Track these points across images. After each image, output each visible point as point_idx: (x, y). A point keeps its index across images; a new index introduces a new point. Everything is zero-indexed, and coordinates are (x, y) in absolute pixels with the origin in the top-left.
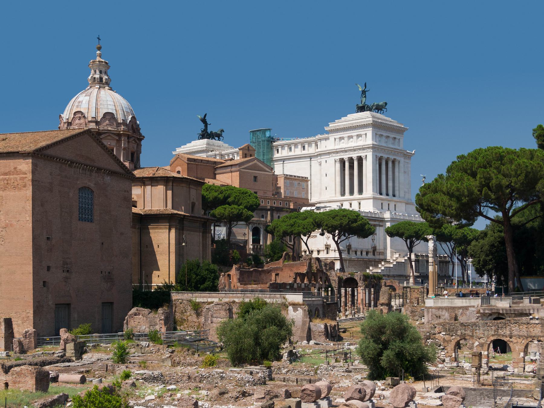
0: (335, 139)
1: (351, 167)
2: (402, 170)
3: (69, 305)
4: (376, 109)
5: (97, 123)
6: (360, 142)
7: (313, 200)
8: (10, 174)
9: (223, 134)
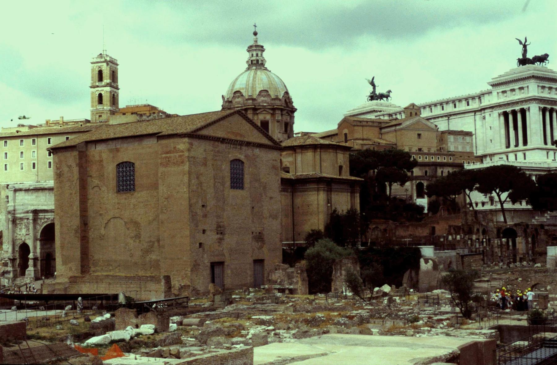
0: (498, 93)
5: (253, 100)
8: (171, 153)
9: (391, 94)
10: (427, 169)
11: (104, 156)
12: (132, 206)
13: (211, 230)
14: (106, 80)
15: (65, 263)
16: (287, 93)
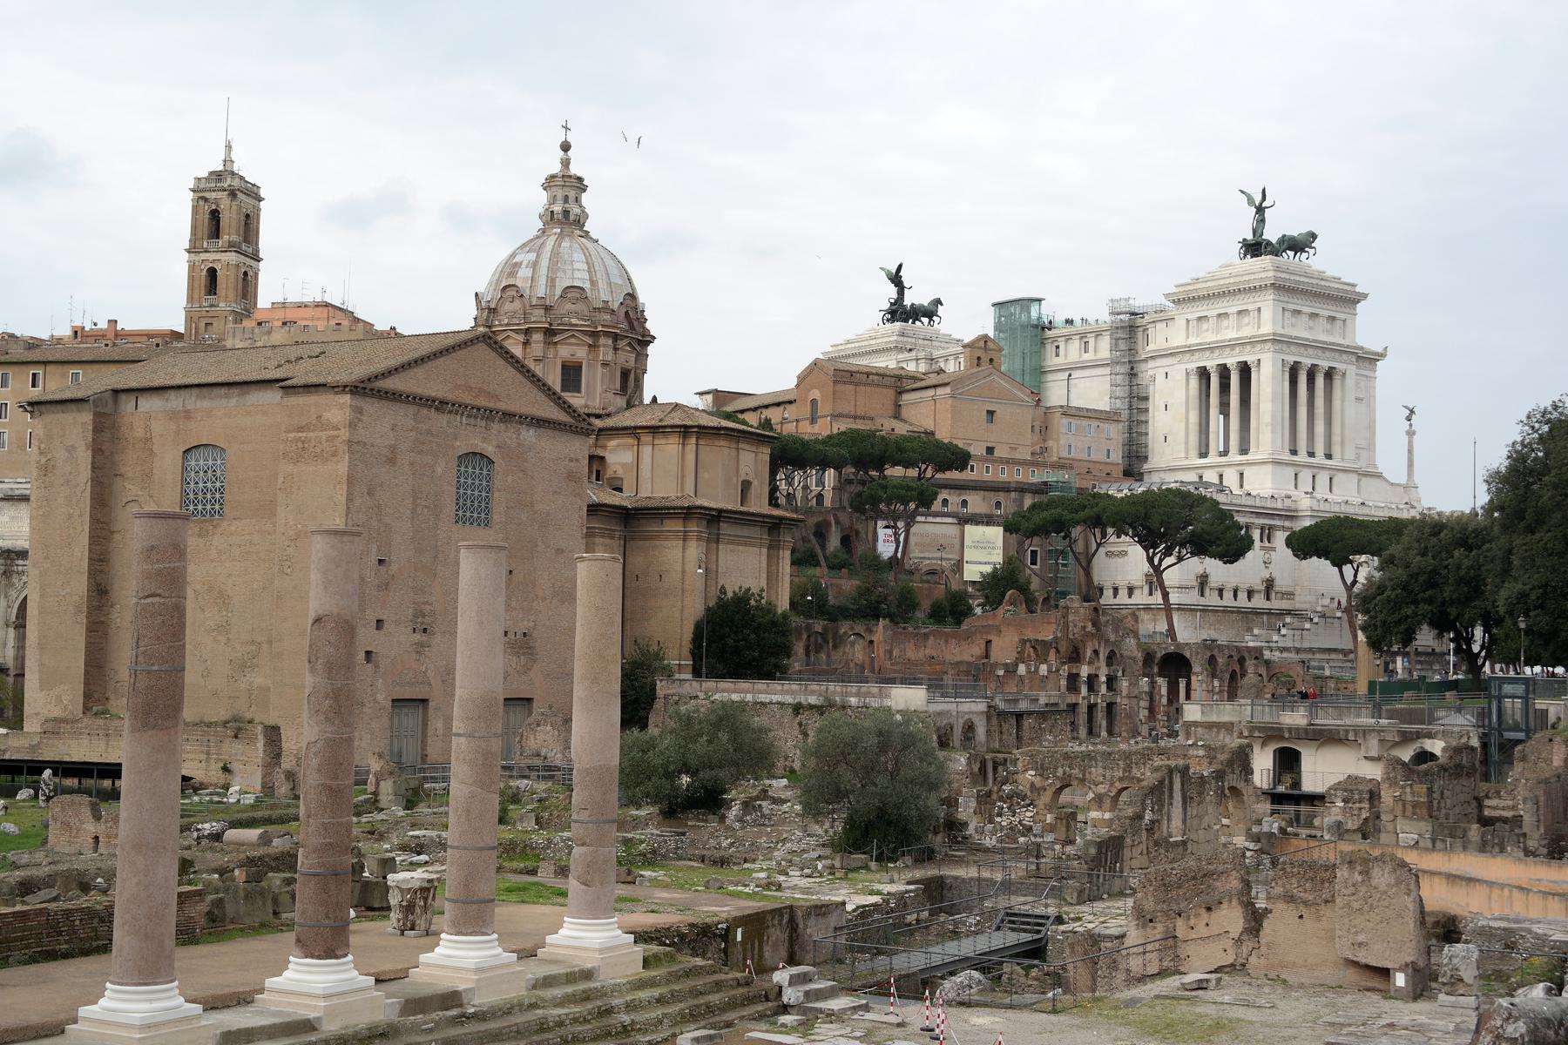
1: (1225, 387)
2: (1351, 394)
5: (548, 309)
6: (1248, 331)
10: (1001, 497)
11: (157, 427)
12: (213, 553)
13: (398, 623)
15: (45, 684)
16: (632, 296)
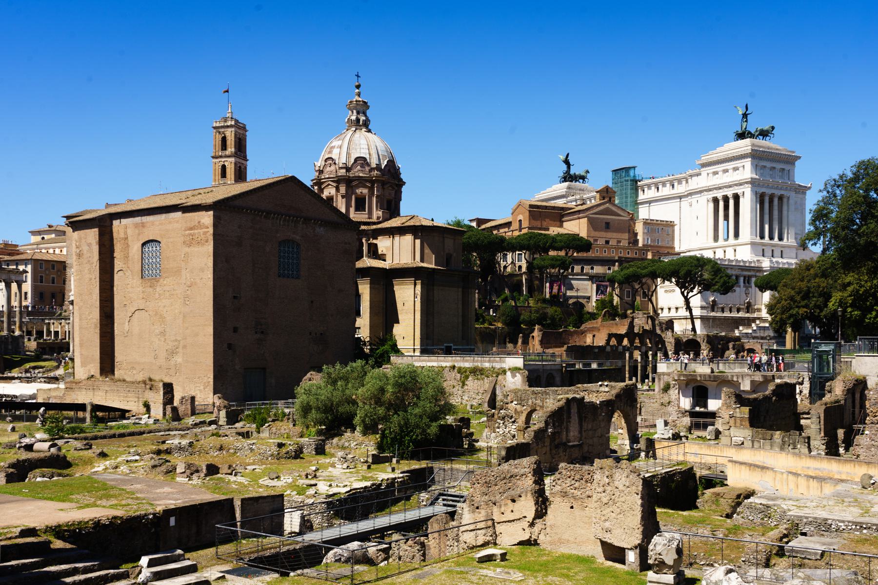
1: (726, 207)
2: (792, 207)
3: (264, 369)
4: (760, 134)
5: (348, 170)
7: (677, 250)
9: (588, 176)
11: (129, 232)
12: (157, 296)
14: (231, 149)
